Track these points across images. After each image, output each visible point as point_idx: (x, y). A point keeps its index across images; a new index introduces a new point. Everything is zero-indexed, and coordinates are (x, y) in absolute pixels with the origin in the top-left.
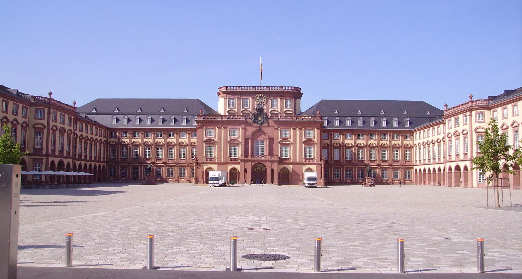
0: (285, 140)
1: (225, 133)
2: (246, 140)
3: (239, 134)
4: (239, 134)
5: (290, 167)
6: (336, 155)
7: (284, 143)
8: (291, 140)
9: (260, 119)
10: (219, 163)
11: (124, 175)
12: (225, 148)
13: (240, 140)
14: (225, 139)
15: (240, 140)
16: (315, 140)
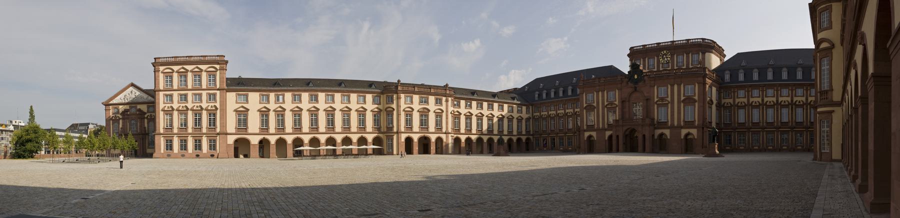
0: (662, 99)
1: (603, 96)
2: (623, 102)
3: (615, 96)
4: (615, 96)
5: (667, 132)
6: (741, 117)
7: (663, 103)
8: (669, 99)
9: (636, 77)
10: (597, 130)
11: (545, 145)
12: (603, 113)
13: (617, 103)
14: (603, 103)
15: (617, 103)
16: (696, 98)
